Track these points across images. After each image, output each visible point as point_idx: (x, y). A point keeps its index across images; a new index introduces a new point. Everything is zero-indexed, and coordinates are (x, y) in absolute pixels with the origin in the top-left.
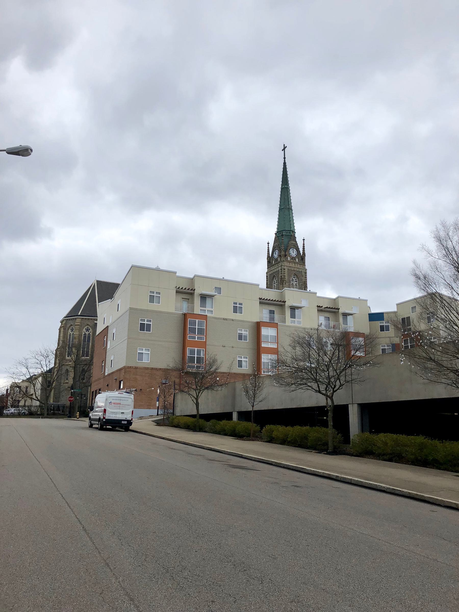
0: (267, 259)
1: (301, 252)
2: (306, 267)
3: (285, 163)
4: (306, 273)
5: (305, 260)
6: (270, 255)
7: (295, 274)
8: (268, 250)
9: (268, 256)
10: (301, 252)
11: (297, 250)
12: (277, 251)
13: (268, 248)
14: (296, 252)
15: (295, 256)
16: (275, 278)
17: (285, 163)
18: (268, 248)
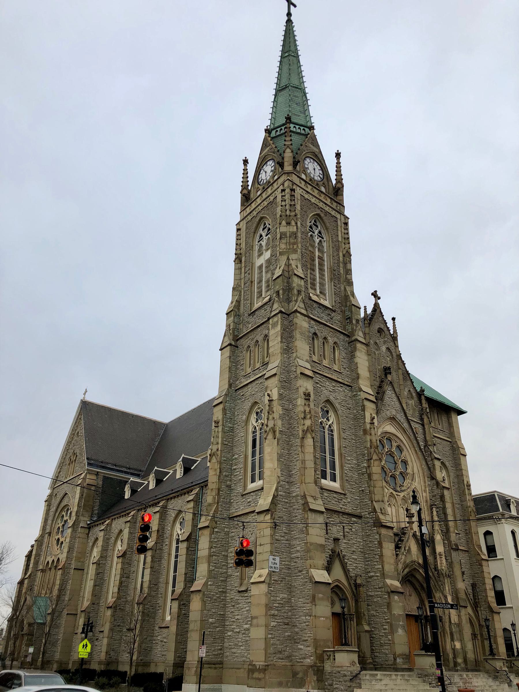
0: (241, 193)
1: (333, 177)
2: (347, 212)
3: (289, 22)
4: (346, 224)
5: (342, 195)
6: (250, 183)
7: (318, 215)
8: (244, 170)
9: (244, 186)
10: (333, 177)
11: (321, 167)
12: (270, 163)
13: (245, 170)
14: (321, 172)
15: (319, 179)
16: (262, 227)
17: (289, 22)
18: (245, 170)
